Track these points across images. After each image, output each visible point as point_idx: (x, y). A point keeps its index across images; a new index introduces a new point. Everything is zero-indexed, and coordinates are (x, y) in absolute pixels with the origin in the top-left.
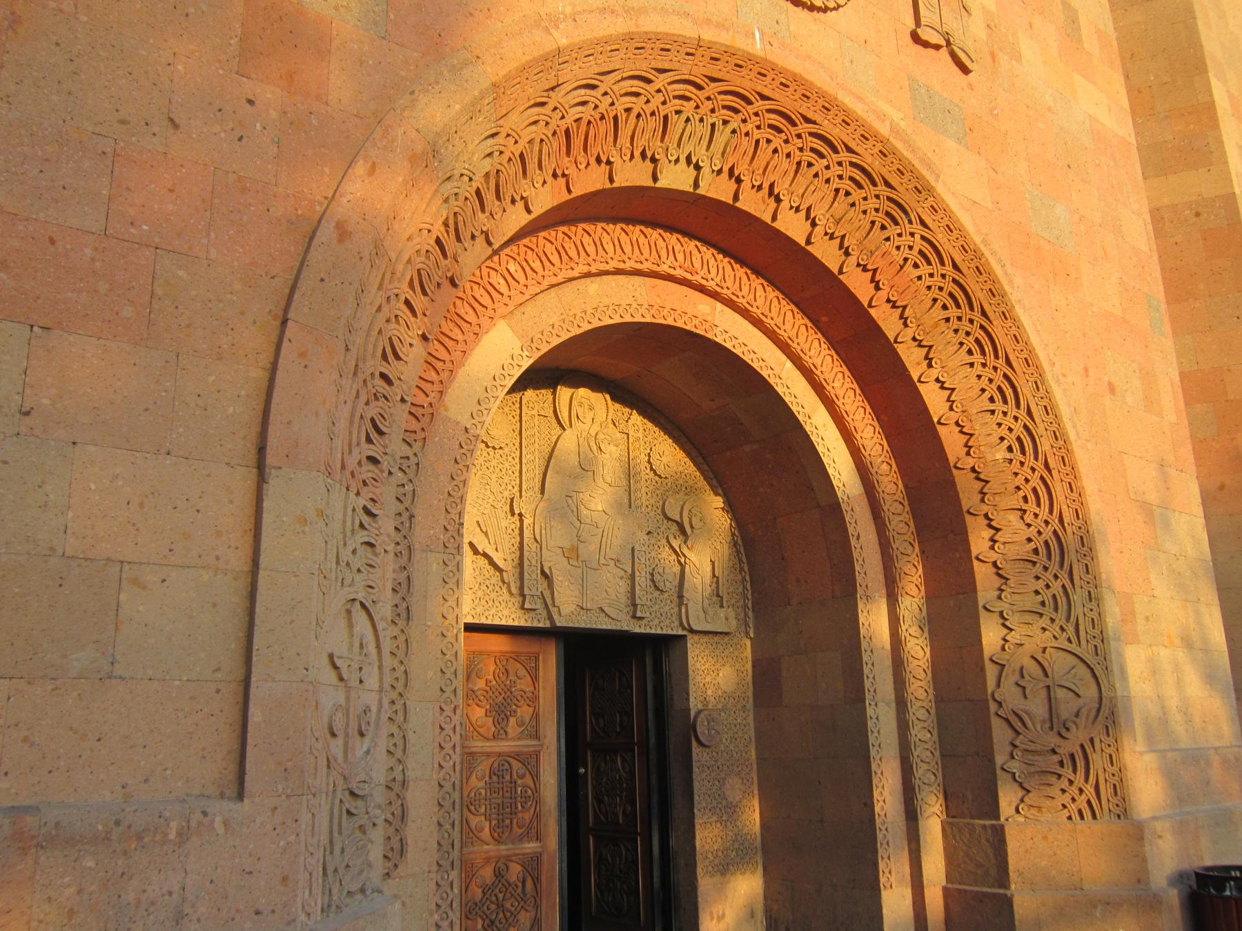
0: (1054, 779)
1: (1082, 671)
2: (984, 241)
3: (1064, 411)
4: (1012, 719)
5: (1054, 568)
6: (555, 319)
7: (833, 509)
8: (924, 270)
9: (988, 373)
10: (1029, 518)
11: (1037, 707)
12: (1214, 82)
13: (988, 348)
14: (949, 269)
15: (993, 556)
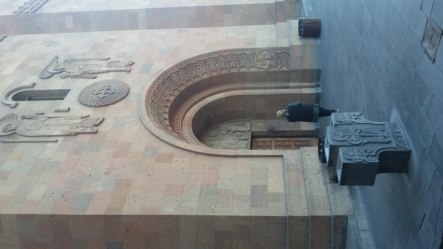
0: (282, 61)
1: (261, 53)
2: (175, 63)
3: (209, 51)
4: (270, 67)
5: (241, 57)
6: (193, 141)
7: (227, 98)
8: (180, 75)
9: (201, 65)
10: (231, 60)
11: (268, 62)
12: (115, 9)
13: (196, 64)
14: (181, 70)
15: (238, 68)
